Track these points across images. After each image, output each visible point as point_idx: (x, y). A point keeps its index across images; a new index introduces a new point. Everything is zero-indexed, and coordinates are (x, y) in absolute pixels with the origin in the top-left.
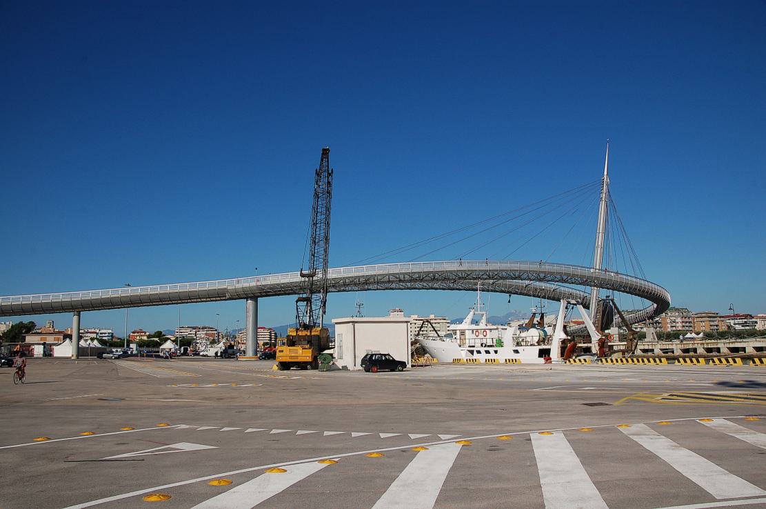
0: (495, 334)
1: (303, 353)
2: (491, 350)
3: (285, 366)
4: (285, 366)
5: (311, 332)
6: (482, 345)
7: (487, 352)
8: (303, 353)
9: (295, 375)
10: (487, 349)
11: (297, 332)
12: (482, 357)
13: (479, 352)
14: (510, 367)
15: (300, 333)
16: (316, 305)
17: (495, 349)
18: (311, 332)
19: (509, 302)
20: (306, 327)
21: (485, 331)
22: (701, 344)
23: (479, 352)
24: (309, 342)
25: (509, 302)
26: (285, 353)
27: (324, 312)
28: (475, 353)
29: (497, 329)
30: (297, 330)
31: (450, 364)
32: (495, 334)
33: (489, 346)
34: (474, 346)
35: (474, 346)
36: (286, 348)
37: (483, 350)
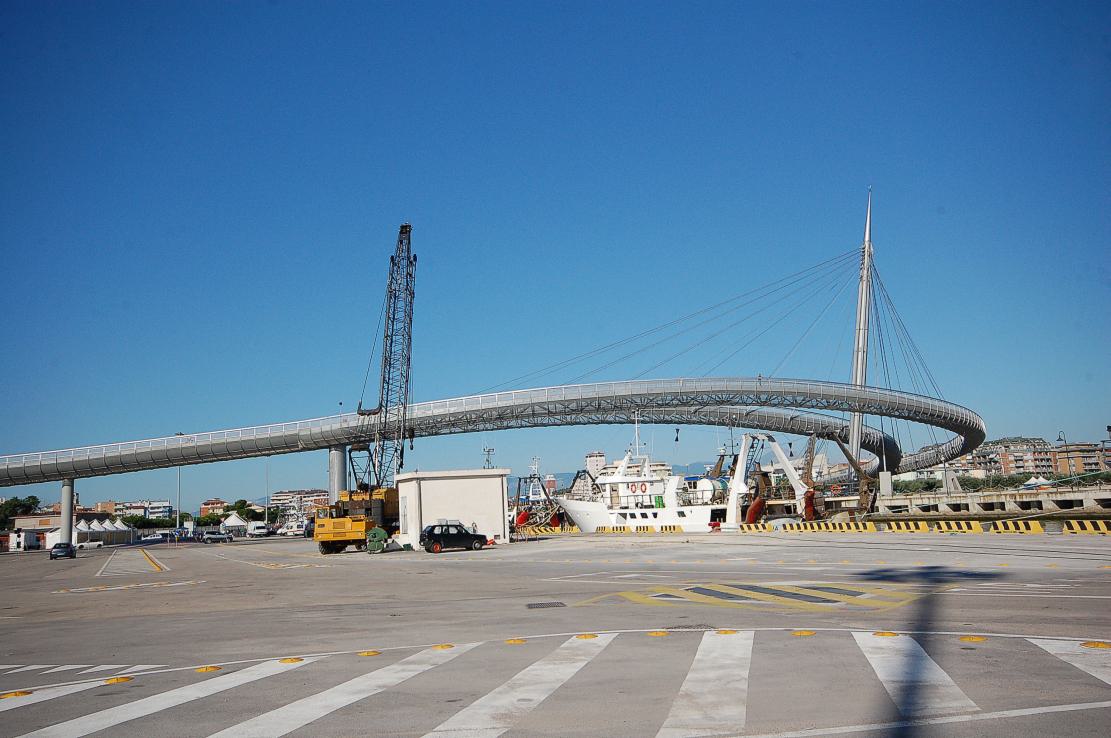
0: (657, 489)
1: (353, 528)
2: (650, 512)
3: (332, 547)
4: (332, 547)
5: (371, 495)
6: (637, 505)
7: (644, 516)
8: (353, 528)
9: (351, 557)
10: (644, 511)
11: (351, 496)
12: (640, 522)
13: (633, 516)
14: (669, 540)
15: (355, 498)
16: (390, 459)
17: (655, 510)
18: (371, 495)
19: (677, 440)
20: (364, 487)
21: (643, 483)
22: (1012, 495)
23: (633, 516)
24: (368, 511)
25: (677, 440)
26: (328, 529)
27: (401, 465)
28: (628, 517)
29: (662, 480)
30: (351, 493)
31: (590, 534)
32: (657, 489)
33: (646, 507)
34: (626, 508)
35: (626, 508)
36: (329, 523)
37: (638, 512)
